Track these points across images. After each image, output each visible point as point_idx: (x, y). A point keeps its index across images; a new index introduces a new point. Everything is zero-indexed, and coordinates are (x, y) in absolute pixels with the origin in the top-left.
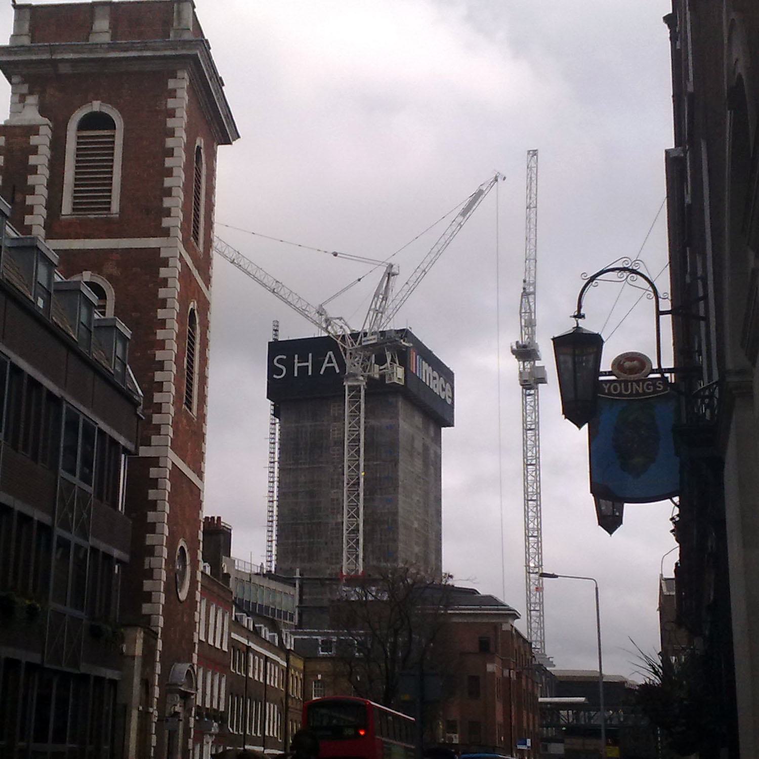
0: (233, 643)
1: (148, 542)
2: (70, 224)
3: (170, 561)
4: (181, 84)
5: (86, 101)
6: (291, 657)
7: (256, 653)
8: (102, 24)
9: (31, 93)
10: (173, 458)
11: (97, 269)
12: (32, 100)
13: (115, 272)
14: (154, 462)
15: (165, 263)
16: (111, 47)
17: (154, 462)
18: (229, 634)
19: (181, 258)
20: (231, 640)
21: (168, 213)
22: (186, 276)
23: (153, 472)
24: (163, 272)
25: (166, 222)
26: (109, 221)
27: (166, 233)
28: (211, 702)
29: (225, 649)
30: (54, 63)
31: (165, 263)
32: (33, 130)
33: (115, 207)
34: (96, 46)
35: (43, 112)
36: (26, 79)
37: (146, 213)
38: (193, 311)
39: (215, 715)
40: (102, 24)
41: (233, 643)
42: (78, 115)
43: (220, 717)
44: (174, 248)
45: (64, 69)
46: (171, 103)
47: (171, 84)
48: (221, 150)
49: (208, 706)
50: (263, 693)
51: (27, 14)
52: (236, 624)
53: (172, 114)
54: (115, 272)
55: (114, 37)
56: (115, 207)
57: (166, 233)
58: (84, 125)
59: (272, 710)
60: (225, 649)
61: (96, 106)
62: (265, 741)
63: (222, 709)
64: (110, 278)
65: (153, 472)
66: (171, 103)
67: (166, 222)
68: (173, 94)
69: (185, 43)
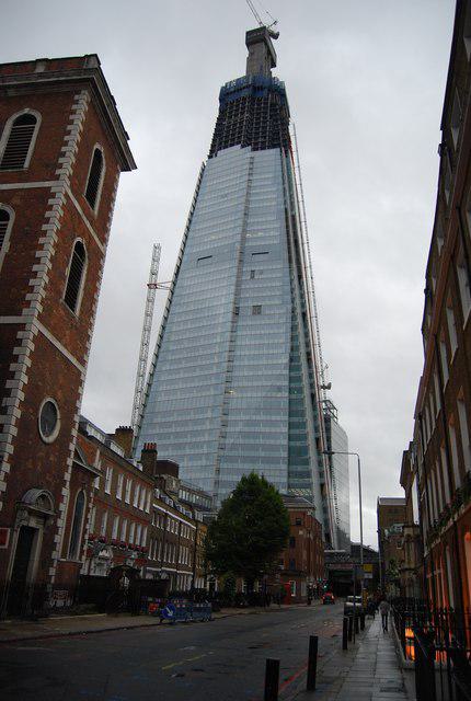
0: (153, 510)
1: (7, 387)
3: (29, 404)
5: (22, 108)
6: (199, 526)
7: (170, 516)
10: (36, 327)
11: (7, 201)
14: (22, 327)
16: (41, 75)
17: (22, 327)
18: (151, 504)
19: (66, 195)
20: (152, 507)
22: (68, 207)
23: (20, 334)
27: (57, 178)
28: (141, 540)
29: (147, 511)
31: (53, 196)
37: (48, 168)
38: (79, 246)
39: (133, 548)
41: (153, 510)
42: (15, 116)
43: (142, 551)
45: (11, 93)
47: (76, 97)
48: (123, 175)
49: (131, 542)
50: (175, 542)
52: (154, 499)
56: (26, 165)
57: (57, 178)
58: (17, 122)
59: (184, 551)
60: (147, 511)
61: (26, 111)
62: (178, 566)
63: (144, 545)
65: (20, 334)
68: (77, 102)
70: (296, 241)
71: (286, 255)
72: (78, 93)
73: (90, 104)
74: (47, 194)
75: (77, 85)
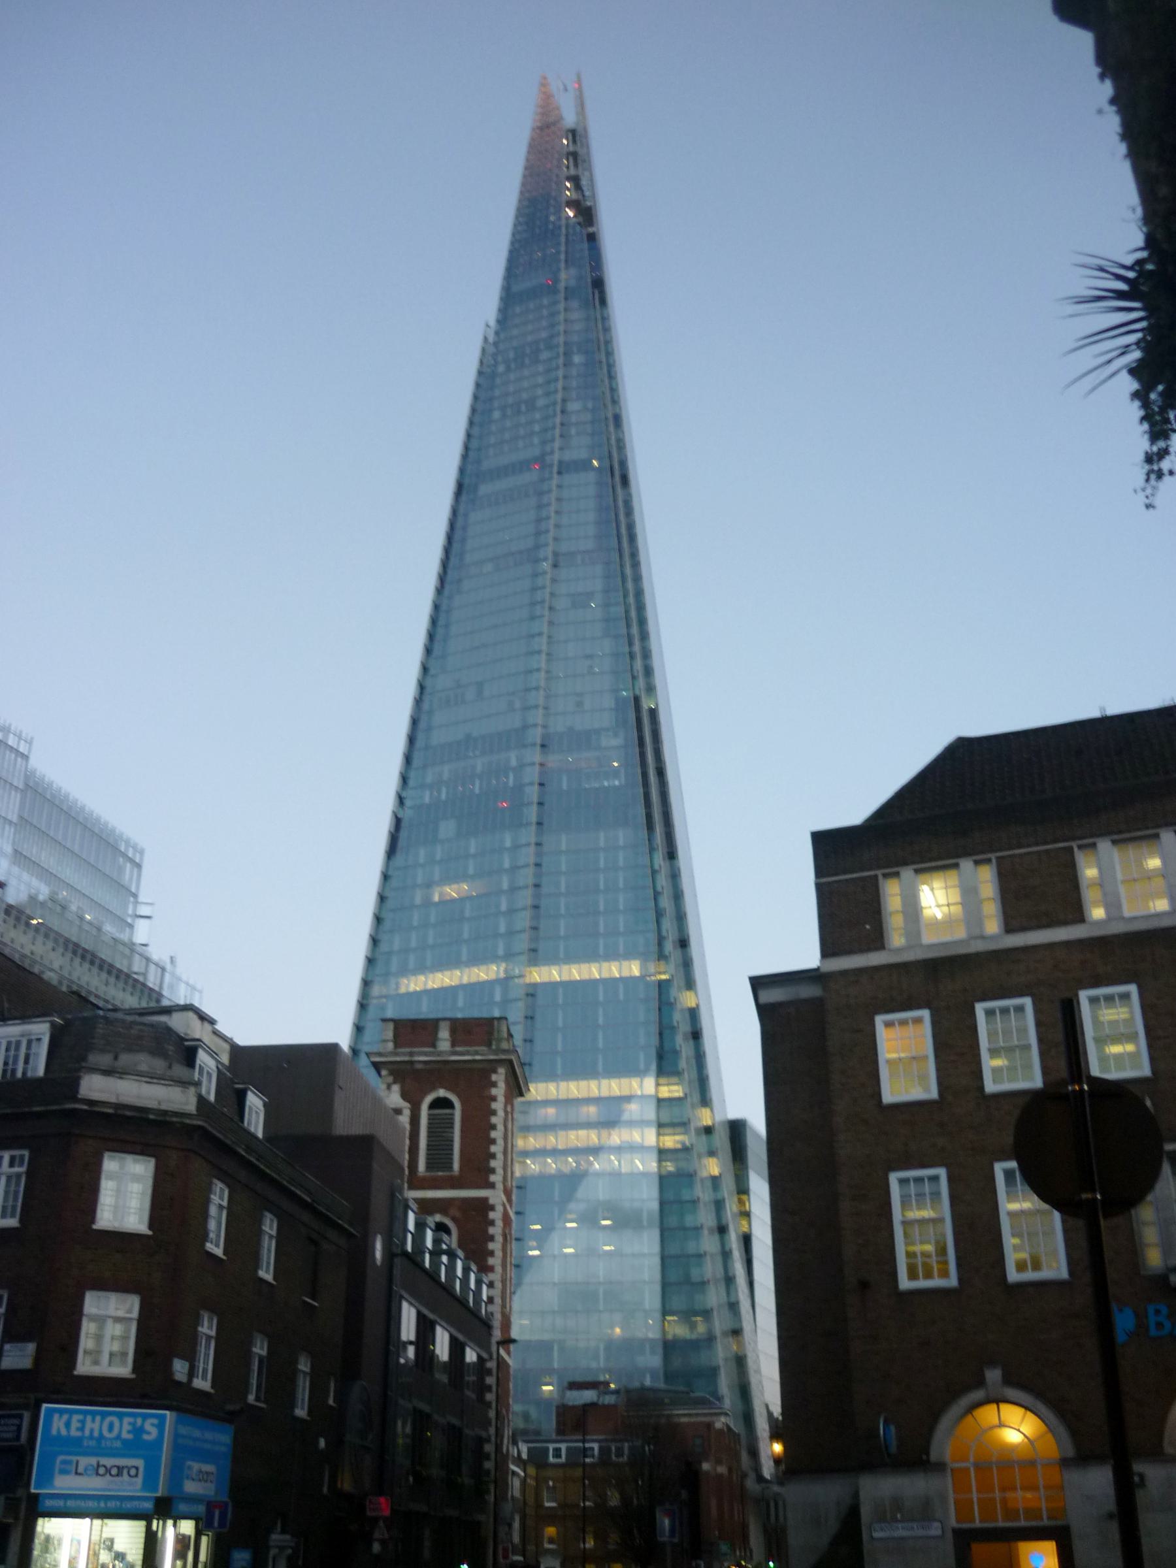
2: (424, 1179)
4: (500, 1077)
5: (433, 1088)
8: (444, 1034)
9: (395, 1082)
11: (444, 1212)
12: (396, 1088)
13: (458, 1214)
15: (492, 1208)
21: (493, 1171)
24: (492, 1215)
25: (492, 1178)
26: (452, 1178)
27: (492, 1186)
30: (412, 1063)
31: (492, 1208)
32: (398, 1111)
33: (456, 1166)
34: (440, 1053)
35: (404, 1096)
36: (391, 1073)
37: (478, 1169)
40: (444, 1034)
44: (496, 1197)
45: (419, 1066)
46: (494, 1091)
47: (494, 1077)
51: (391, 1026)
53: (494, 1099)
54: (458, 1214)
55: (453, 1045)
56: (456, 1166)
57: (492, 1186)
61: (442, 1093)
64: (454, 1219)
66: (494, 1091)
67: (492, 1178)
68: (494, 1085)
69: (505, 1051)
70: (661, 772)
71: (641, 811)
72: (495, 1072)
73: (507, 1082)
74: (484, 1206)
75: (492, 1066)
